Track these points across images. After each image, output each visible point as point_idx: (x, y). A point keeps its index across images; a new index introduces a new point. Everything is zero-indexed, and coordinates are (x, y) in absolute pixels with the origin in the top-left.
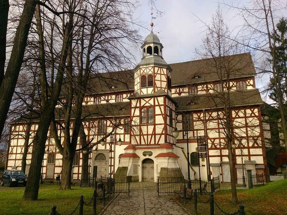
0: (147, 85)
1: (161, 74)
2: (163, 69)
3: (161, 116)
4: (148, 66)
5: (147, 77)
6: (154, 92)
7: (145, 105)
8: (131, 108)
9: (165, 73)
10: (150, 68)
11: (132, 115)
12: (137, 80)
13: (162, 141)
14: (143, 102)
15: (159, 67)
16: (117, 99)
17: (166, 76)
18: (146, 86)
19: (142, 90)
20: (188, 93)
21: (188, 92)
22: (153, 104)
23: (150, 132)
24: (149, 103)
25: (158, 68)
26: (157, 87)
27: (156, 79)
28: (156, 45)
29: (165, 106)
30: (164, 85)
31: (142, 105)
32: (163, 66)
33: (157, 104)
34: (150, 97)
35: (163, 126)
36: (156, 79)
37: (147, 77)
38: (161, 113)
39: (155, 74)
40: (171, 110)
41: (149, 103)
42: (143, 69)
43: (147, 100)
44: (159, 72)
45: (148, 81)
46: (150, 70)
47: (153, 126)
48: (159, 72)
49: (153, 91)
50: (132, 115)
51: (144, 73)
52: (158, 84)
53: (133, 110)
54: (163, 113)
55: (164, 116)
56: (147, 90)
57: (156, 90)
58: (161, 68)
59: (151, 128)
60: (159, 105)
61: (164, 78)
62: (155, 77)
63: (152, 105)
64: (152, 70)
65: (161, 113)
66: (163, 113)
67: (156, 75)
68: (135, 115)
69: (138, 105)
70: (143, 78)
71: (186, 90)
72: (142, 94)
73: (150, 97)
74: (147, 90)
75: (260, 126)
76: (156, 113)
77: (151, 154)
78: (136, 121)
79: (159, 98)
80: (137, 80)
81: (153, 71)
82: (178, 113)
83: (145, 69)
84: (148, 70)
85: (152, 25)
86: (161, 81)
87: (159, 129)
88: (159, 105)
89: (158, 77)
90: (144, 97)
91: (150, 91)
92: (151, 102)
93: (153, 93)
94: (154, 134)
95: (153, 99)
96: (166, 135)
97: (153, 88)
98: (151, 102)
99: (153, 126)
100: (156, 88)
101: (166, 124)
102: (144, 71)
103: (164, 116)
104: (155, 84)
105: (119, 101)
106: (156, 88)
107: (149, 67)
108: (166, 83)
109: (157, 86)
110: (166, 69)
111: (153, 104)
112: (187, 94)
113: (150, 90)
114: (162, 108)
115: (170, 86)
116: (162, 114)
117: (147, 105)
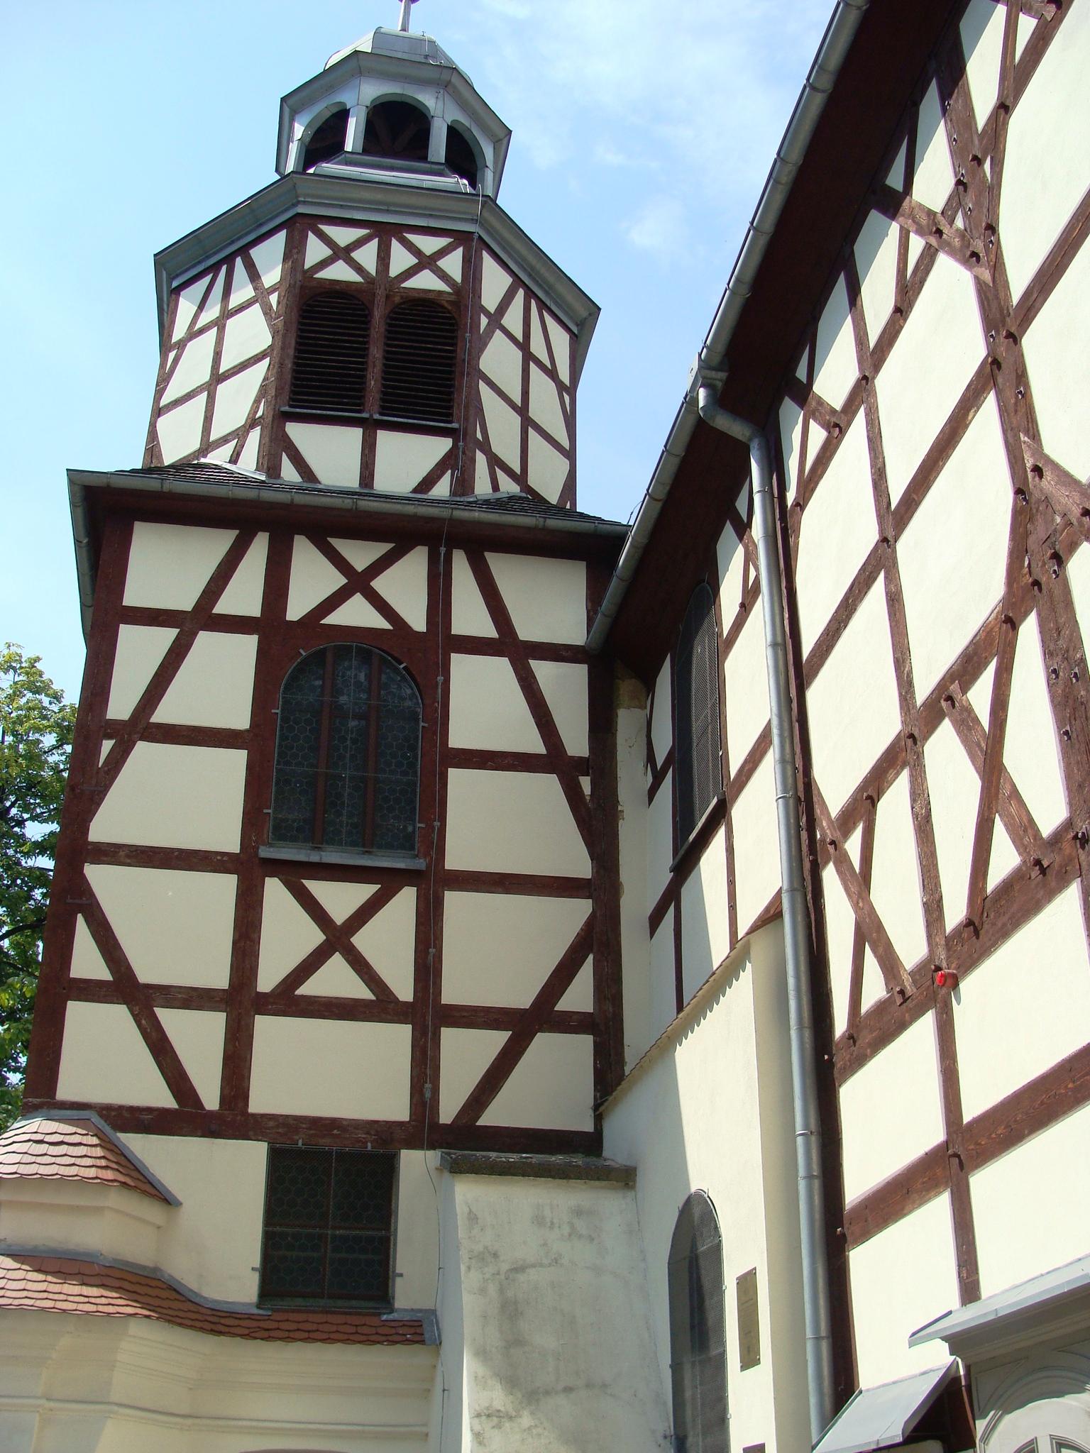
5: (378, 315)
6: (454, 493)
18: (357, 401)
19: (308, 437)
37: (378, 315)
39: (484, 321)
43: (360, 555)
73: (398, 528)
81: (457, 276)
89: (498, 360)
93: (442, 489)
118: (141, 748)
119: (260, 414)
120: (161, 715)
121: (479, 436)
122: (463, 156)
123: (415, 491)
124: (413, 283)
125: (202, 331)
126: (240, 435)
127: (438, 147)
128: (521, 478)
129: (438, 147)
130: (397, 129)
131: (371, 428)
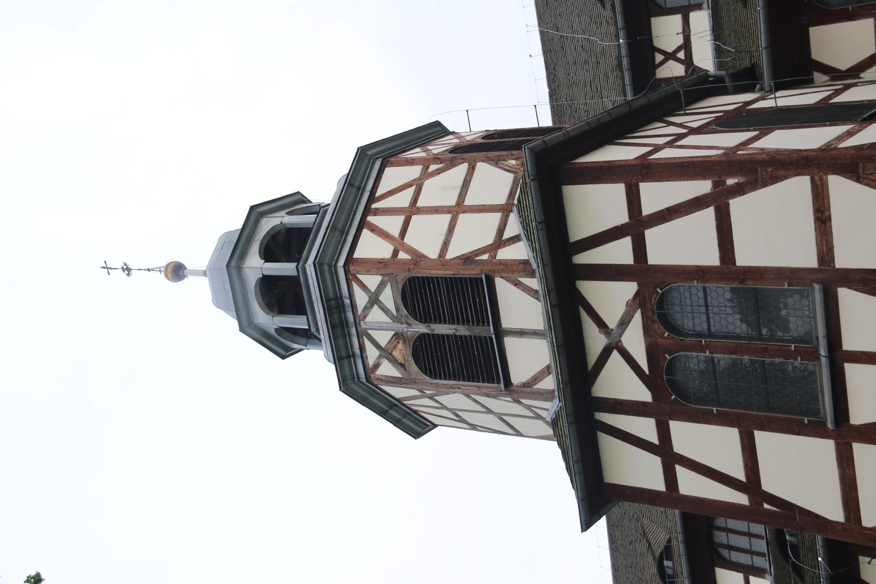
0: (479, 331)
1: (413, 210)
2: (379, 193)
3: (737, 205)
4: (350, 315)
6: (532, 275)
7: (643, 362)
8: (671, 495)
9: (414, 172)
10: (361, 299)
11: (742, 499)
14: (619, 382)
15: (362, 224)
16: (745, 559)
17: (433, 168)
18: (484, 343)
19: (519, 374)
20: (694, 16)
21: (685, 12)
22: (630, 288)
24: (624, 323)
25: (365, 232)
26: (500, 242)
27: (432, 253)
28: (255, 248)
31: (643, 394)
32: (361, 189)
33: (620, 252)
35: (837, 184)
36: (432, 253)
38: (708, 215)
39: (402, 255)
41: (624, 323)
42: (372, 354)
43: (595, 341)
44: (392, 224)
46: (374, 300)
47: (847, 297)
48: (392, 224)
49: (517, 284)
50: (742, 499)
51: (396, 354)
52: (474, 234)
53: (691, 484)
54: (704, 187)
55: (730, 182)
56: (521, 333)
57: (519, 252)
58: (367, 211)
60: (637, 226)
62: (418, 257)
63: (639, 301)
64: (372, 281)
65: (708, 215)
66: (704, 187)
67: (410, 250)
68: (740, 474)
69: (645, 428)
71: (666, 31)
72: (549, 383)
73: (567, 314)
74: (521, 333)
76: (711, 258)
79: (579, 231)
81: (378, 279)
82: (796, 67)
83: (368, 345)
84: (376, 315)
85: (177, 271)
86: (458, 209)
88: (637, 226)
89: (426, 238)
92: (611, 299)
93: (533, 283)
95: (590, 289)
97: (502, 287)
98: (611, 299)
99: (847, 297)
100: (505, 254)
101: (816, 165)
102: (386, 353)
103: (730, 182)
104: (468, 259)
105: (761, 545)
106: (505, 254)
107: (353, 306)
108: (482, 168)
109: (489, 239)
110: (388, 171)
111: (630, 288)
112: (701, 21)
113: (521, 307)
114: (656, 196)
116: (719, 203)
117: (635, 340)
118: (768, 485)
119: (510, 399)
120: (740, 474)
121: (485, 257)
122: (285, 244)
123: (537, 299)
124: (391, 307)
125: (457, 416)
126: (529, 407)
127: (286, 268)
128: (505, 210)
129: (286, 268)
130: (281, 295)
131: (500, 333)
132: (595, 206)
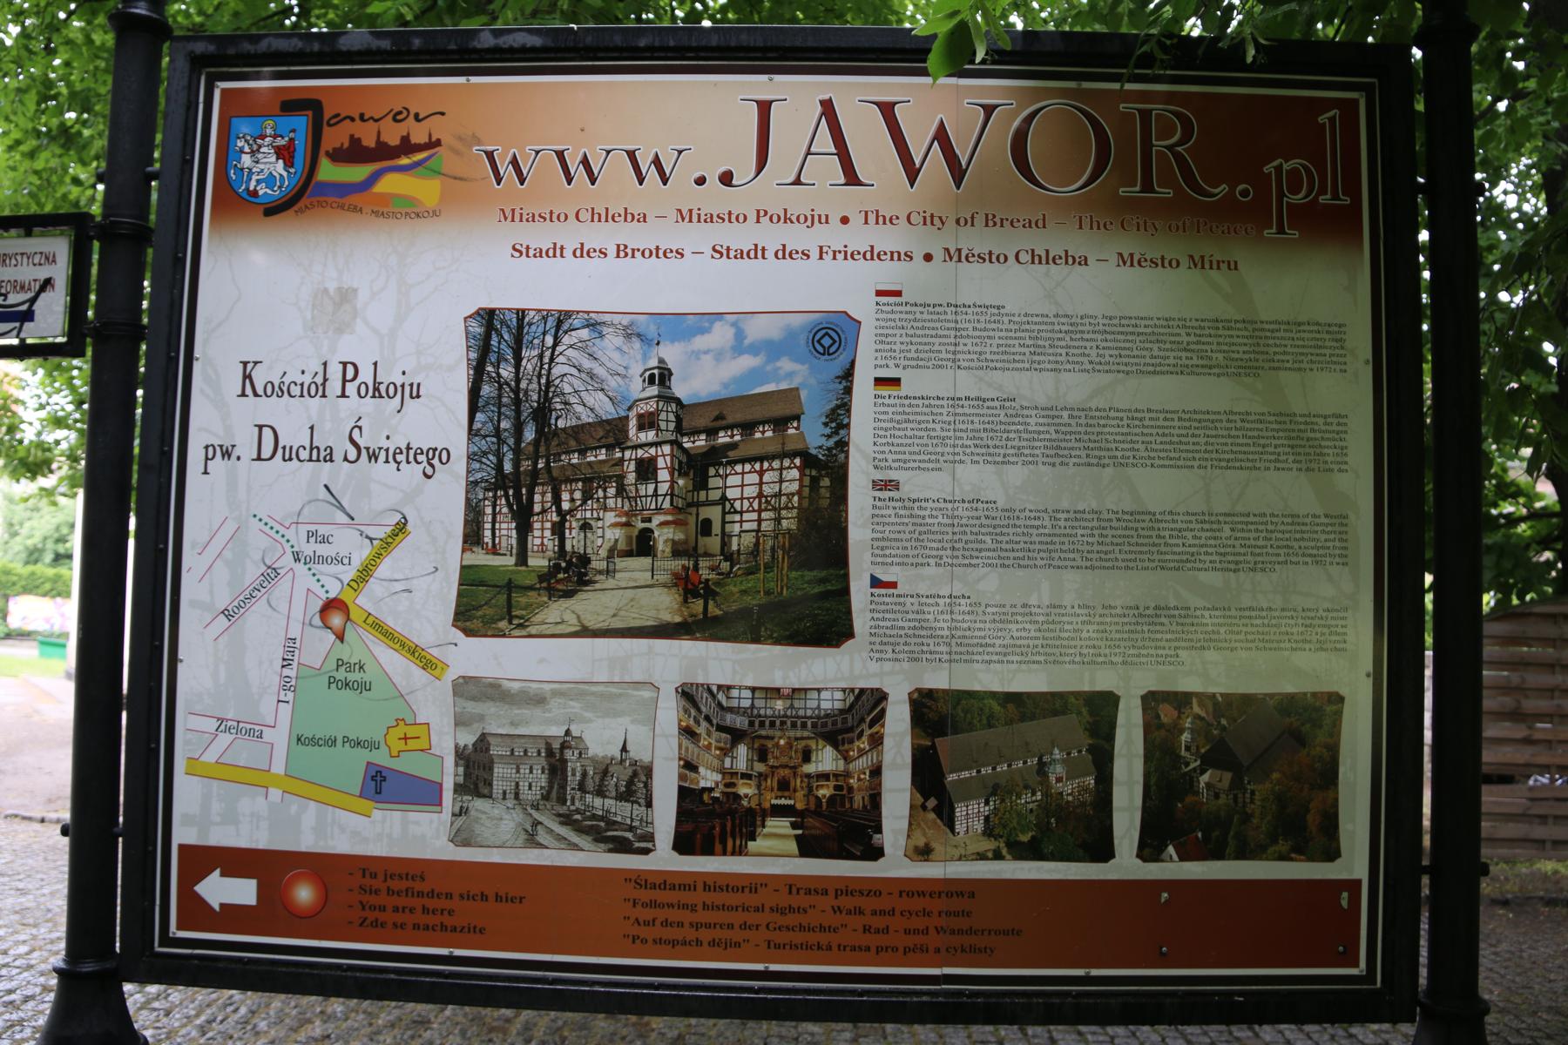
12: (633, 423)
13: (667, 505)
14: (640, 452)
23: (650, 492)
29: (672, 456)
30: (672, 426)
34: (651, 445)
40: (680, 463)
45: (647, 422)
52: (663, 425)
59: (651, 488)
61: (672, 417)
70: (640, 416)
73: (651, 445)
75: (801, 480)
77: (649, 520)
78: (631, 478)
80: (633, 423)
87: (664, 488)
89: (663, 416)
90: (641, 446)
91: (650, 436)
92: (652, 451)
94: (656, 494)
96: (672, 495)
115: (679, 429)
132: (667, 449)
